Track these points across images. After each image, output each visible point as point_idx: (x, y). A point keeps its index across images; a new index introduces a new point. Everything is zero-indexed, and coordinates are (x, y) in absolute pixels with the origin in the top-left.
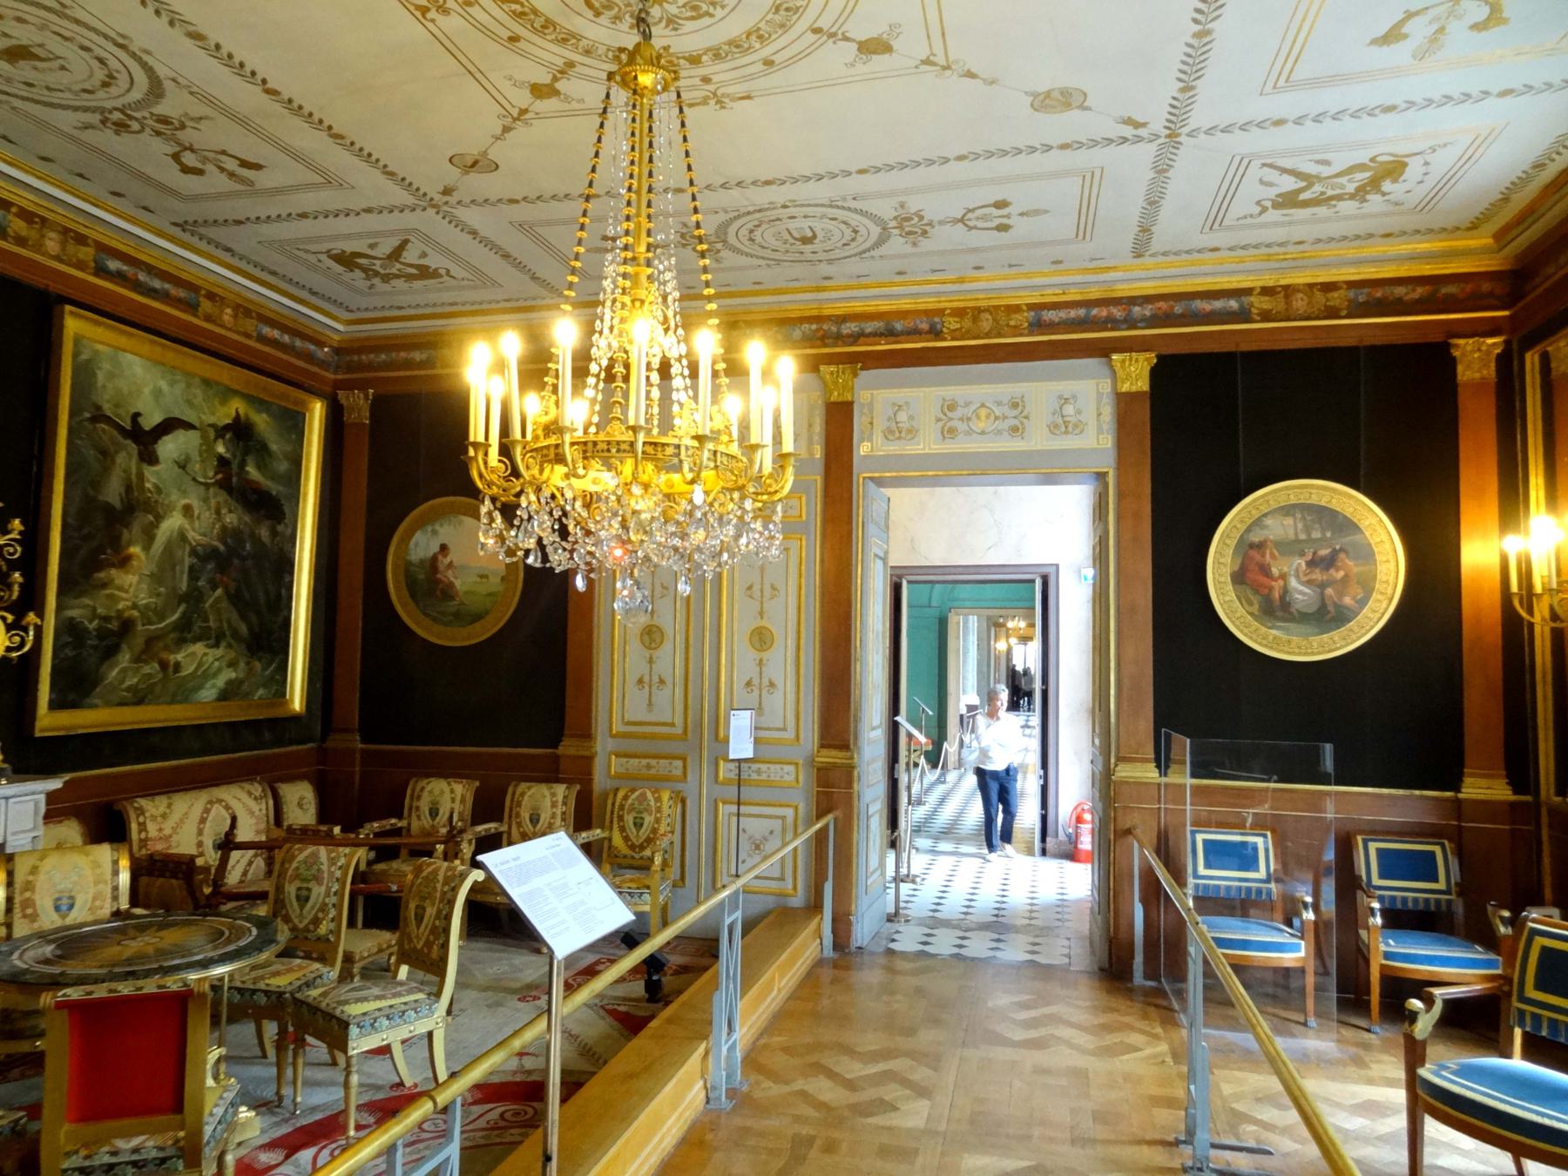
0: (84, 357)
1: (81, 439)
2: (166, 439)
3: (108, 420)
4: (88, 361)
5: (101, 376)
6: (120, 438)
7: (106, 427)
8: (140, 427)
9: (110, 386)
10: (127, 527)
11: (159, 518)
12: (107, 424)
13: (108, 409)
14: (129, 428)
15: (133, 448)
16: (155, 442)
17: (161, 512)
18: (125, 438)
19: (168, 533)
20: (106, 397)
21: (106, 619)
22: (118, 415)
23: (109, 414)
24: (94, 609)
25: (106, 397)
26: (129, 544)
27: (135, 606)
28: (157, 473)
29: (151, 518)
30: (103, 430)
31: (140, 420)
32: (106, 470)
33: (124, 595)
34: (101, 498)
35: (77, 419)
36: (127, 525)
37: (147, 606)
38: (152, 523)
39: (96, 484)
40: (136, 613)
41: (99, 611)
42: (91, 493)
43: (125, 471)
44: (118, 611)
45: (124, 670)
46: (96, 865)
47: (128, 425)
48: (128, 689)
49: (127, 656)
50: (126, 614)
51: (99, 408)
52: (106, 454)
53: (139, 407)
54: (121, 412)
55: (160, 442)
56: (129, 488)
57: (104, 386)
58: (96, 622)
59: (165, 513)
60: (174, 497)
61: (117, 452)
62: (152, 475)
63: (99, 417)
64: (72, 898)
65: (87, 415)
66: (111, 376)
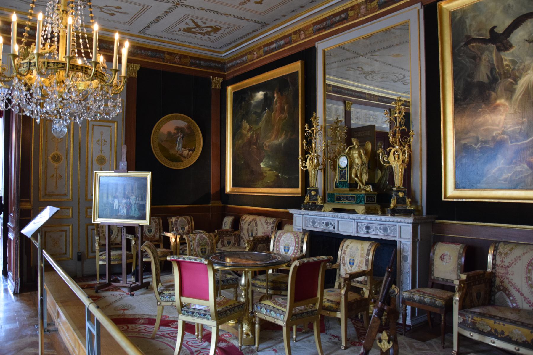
0: (458, 17)
1: (460, 56)
2: (516, 31)
3: (476, 40)
4: (461, 18)
5: (468, 22)
6: (484, 46)
7: (474, 44)
8: (496, 33)
9: (474, 23)
10: (494, 91)
11: (516, 79)
12: (474, 42)
13: (474, 35)
14: (488, 37)
15: (493, 47)
16: (509, 36)
17: (517, 74)
18: (486, 45)
19: (525, 85)
20: (473, 29)
21: (485, 142)
22: (481, 35)
23: (475, 37)
24: (477, 138)
25: (473, 29)
26: (496, 99)
27: (504, 133)
28: (512, 53)
29: (510, 80)
30: (473, 47)
31: (495, 30)
32: (477, 66)
33: (495, 128)
34: (475, 81)
35: (458, 48)
36: (494, 90)
37: (513, 132)
38: (511, 82)
39: (471, 76)
40: (506, 137)
41: (480, 138)
42: (469, 80)
43: (489, 61)
44: (494, 137)
45: (500, 169)
46: (363, 249)
47: (488, 37)
48: (506, 180)
49: (502, 161)
50: (499, 138)
51: (468, 37)
52: (475, 58)
53: (495, 23)
54: (483, 32)
55: (512, 35)
56: (492, 70)
57: (471, 25)
58: (479, 144)
59: (521, 74)
60: (527, 63)
61: (482, 54)
62: (507, 57)
63: (470, 40)
64: (354, 260)
65: (463, 44)
66: (474, 17)
